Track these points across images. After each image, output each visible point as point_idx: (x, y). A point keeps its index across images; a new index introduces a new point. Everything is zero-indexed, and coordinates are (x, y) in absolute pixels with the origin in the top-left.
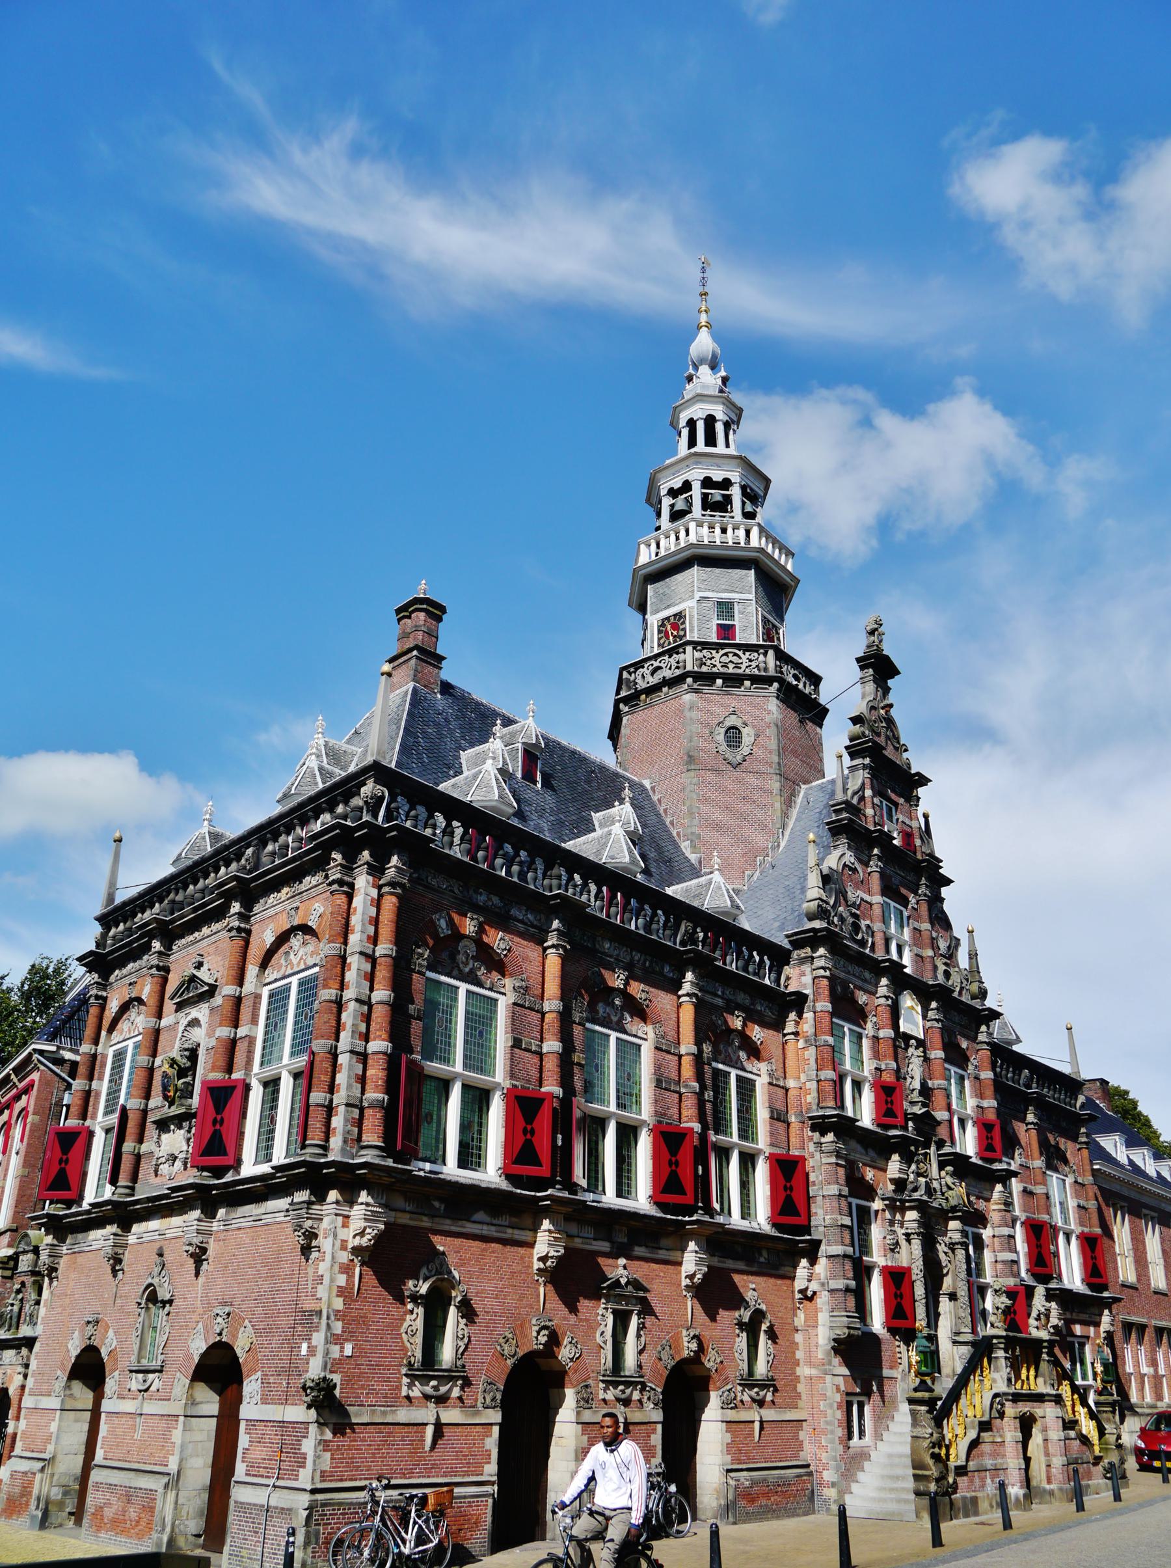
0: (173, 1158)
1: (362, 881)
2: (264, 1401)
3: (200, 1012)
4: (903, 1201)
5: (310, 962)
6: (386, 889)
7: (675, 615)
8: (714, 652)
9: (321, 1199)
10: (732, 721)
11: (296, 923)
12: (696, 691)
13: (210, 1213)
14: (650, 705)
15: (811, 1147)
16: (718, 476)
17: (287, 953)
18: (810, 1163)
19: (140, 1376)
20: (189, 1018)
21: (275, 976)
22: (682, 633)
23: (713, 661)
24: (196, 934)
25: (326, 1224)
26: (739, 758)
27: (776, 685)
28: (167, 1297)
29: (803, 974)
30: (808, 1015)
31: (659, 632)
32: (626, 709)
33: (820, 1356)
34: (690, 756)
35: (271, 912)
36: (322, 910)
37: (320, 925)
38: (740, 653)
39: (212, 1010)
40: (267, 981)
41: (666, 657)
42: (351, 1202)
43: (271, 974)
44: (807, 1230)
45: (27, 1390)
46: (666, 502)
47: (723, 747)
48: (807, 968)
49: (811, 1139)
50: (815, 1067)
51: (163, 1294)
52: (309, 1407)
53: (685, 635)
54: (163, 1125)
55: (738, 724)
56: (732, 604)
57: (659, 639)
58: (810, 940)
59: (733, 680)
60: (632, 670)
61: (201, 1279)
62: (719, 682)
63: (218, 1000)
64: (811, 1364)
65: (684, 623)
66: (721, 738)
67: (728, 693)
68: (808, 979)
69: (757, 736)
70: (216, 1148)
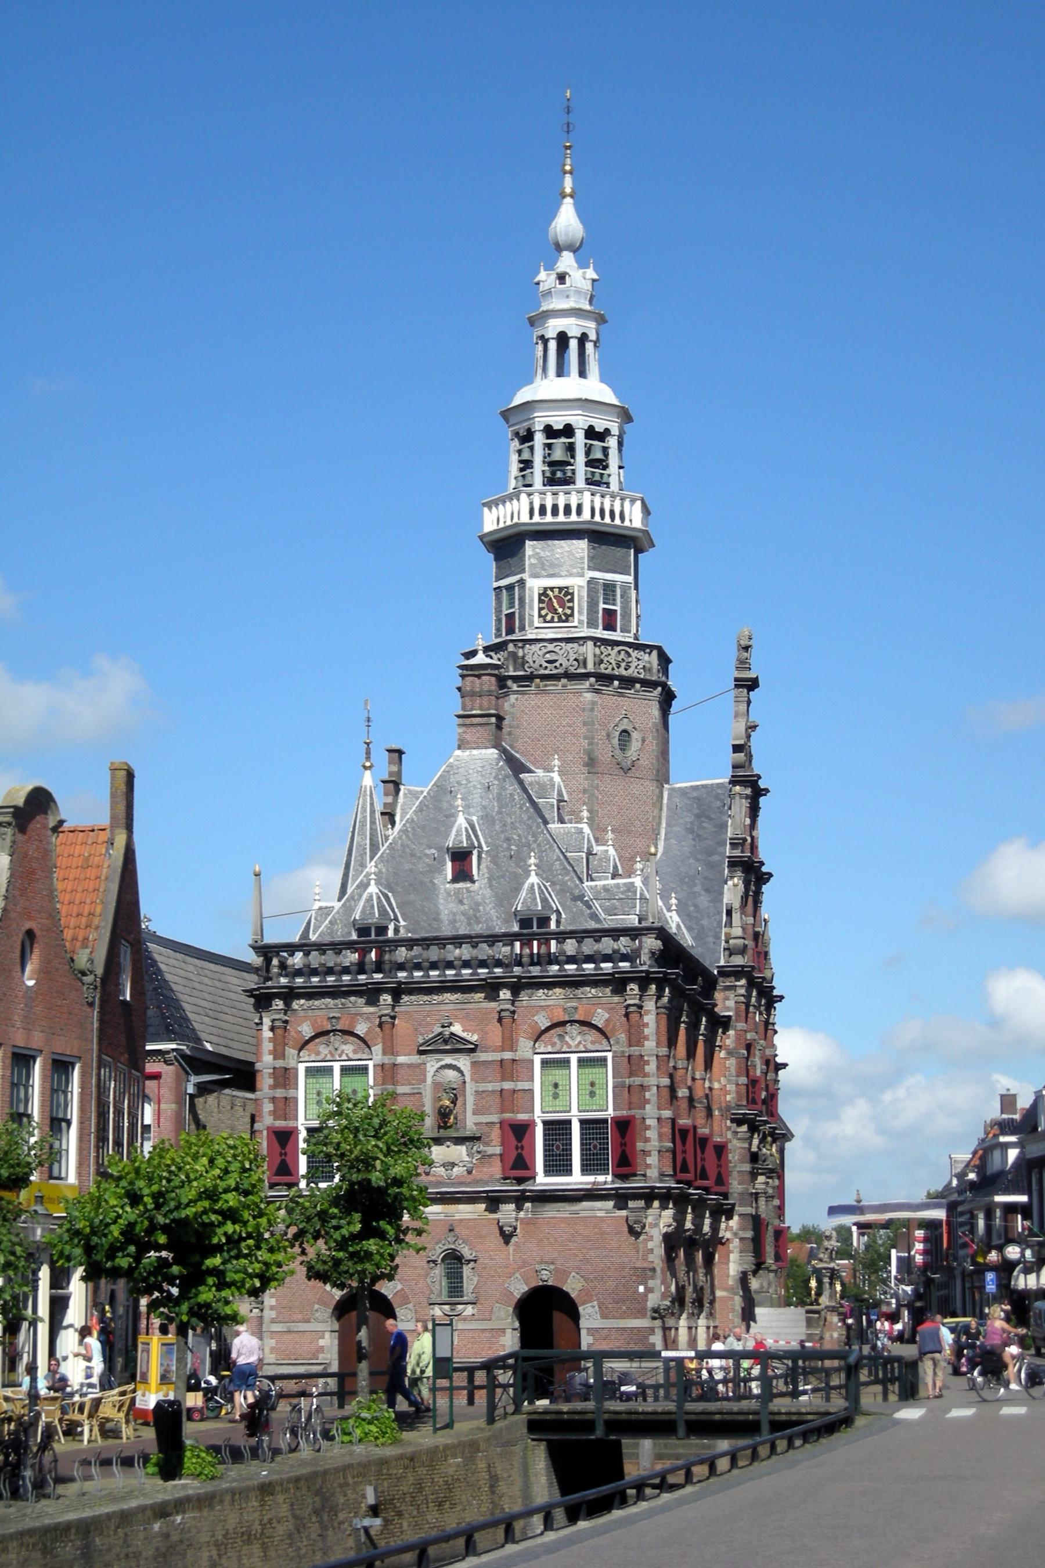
0: (450, 1165)
1: (650, 1005)
2: (604, 1316)
3: (463, 1062)
4: (758, 1169)
5: (590, 1047)
6: (663, 1010)
7: (561, 589)
8: (609, 648)
9: (649, 1206)
10: (625, 725)
11: (577, 1017)
12: (597, 691)
13: (519, 1208)
14: (545, 692)
15: (729, 1135)
16: (600, 426)
17: (561, 1037)
18: (730, 1146)
19: (447, 1307)
20: (443, 1063)
21: (550, 1049)
22: (568, 612)
23: (609, 659)
24: (436, 997)
25: (650, 1219)
26: (629, 763)
27: (660, 689)
28: (471, 1258)
29: (727, 998)
30: (731, 1032)
31: (540, 601)
32: (515, 687)
33: (731, 1282)
34: (590, 759)
35: (543, 1003)
36: (607, 1016)
37: (606, 1026)
38: (630, 650)
39: (474, 1064)
40: (538, 1051)
41: (563, 645)
42: (664, 1207)
43: (541, 1047)
44: (726, 1196)
45: (266, 1320)
46: (539, 439)
47: (618, 752)
48: (731, 994)
49: (729, 1128)
50: (734, 1074)
51: (466, 1252)
52: (654, 1318)
53: (572, 615)
54: (438, 1141)
55: (629, 728)
56: (614, 586)
57: (540, 609)
58: (738, 973)
59: (628, 682)
60: (520, 645)
61: (511, 1247)
62: (616, 683)
63: (482, 1056)
64: (724, 1289)
65: (571, 600)
66: (616, 741)
67: (621, 695)
68: (731, 1003)
69: (643, 741)
70: (519, 1165)
